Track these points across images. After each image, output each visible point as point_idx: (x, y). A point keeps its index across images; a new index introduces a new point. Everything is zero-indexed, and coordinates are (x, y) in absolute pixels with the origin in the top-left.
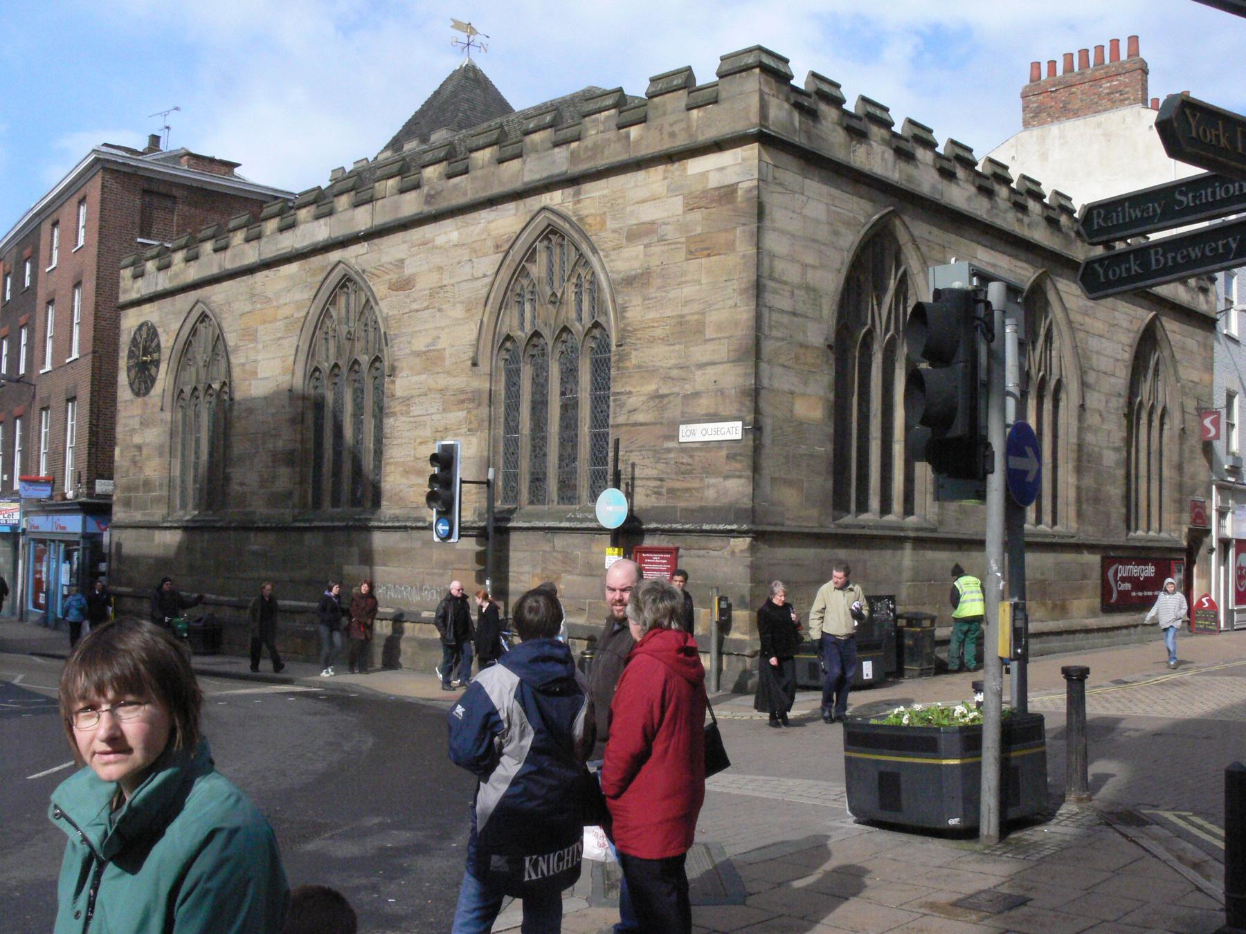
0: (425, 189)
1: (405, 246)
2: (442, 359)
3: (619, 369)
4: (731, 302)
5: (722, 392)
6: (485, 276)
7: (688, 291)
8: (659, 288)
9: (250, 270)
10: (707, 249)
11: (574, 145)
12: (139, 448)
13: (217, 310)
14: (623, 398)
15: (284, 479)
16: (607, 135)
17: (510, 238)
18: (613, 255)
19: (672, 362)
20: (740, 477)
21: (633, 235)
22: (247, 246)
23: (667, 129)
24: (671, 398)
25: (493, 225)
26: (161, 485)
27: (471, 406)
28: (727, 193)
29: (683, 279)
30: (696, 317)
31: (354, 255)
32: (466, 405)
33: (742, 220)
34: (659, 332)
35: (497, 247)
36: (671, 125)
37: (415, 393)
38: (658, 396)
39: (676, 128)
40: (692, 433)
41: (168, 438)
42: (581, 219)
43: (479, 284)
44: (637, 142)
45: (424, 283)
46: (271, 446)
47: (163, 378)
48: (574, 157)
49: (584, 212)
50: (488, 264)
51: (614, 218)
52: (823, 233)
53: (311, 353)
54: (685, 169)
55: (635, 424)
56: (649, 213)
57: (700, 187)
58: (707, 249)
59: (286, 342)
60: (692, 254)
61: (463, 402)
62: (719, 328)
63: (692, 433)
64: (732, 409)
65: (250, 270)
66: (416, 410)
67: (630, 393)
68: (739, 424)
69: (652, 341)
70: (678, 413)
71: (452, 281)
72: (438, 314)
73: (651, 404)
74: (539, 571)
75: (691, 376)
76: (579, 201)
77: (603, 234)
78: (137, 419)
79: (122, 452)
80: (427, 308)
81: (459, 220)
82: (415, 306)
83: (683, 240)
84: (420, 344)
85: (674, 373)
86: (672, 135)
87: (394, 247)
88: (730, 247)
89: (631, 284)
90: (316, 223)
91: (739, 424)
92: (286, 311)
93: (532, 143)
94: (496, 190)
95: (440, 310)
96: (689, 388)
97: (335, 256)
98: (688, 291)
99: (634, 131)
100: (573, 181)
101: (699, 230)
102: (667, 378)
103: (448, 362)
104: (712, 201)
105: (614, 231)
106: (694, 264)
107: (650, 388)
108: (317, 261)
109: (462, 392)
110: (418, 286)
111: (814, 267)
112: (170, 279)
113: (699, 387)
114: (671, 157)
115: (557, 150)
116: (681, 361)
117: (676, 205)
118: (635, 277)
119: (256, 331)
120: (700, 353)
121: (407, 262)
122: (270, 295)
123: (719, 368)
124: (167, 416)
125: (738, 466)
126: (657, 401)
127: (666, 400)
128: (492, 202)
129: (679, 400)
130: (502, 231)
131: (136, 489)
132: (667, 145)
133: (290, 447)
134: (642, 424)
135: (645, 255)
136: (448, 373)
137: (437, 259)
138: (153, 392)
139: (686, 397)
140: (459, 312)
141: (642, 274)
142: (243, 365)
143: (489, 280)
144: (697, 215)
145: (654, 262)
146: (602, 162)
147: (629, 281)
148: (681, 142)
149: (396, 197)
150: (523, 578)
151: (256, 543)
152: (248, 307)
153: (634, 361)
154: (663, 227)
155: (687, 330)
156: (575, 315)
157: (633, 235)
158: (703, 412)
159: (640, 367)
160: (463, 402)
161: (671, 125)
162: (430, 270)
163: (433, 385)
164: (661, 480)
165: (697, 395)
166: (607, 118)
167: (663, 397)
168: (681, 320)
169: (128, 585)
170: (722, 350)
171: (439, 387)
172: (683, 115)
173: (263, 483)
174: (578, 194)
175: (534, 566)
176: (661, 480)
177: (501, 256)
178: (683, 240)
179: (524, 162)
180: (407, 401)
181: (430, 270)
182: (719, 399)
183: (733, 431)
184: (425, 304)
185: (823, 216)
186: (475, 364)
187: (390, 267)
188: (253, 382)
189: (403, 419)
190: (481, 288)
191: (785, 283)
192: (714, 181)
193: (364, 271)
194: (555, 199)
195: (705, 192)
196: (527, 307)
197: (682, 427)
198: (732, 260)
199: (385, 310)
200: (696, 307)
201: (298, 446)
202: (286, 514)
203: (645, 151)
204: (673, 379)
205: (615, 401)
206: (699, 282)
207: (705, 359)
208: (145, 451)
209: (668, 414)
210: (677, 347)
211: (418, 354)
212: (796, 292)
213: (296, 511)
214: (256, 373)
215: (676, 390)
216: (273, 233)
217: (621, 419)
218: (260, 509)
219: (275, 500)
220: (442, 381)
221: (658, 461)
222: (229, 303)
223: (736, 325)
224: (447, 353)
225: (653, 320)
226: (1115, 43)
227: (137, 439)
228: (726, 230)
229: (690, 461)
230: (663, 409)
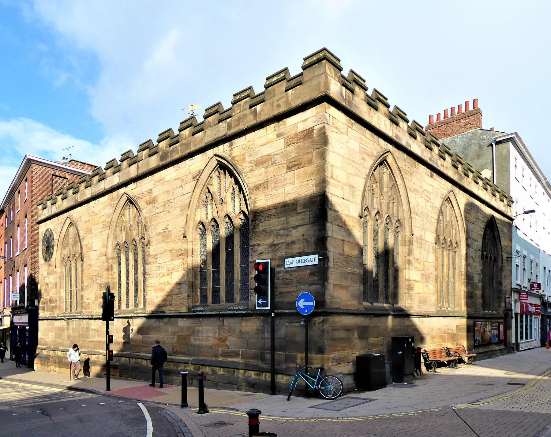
0: (160, 153)
1: (153, 182)
3: (253, 233)
6: (188, 193)
10: (298, 165)
12: (47, 285)
13: (75, 221)
14: (255, 247)
17: (200, 172)
18: (249, 174)
24: (280, 245)
25: (191, 167)
28: (308, 133)
29: (285, 183)
31: (130, 189)
34: (273, 212)
35: (194, 178)
38: (274, 245)
40: (292, 263)
42: (233, 158)
43: (185, 197)
45: (161, 200)
47: (57, 254)
51: (250, 155)
52: (357, 157)
56: (266, 151)
58: (298, 165)
59: (104, 233)
60: (289, 168)
63: (292, 263)
67: (259, 244)
69: (270, 217)
70: (283, 253)
71: (174, 197)
72: (168, 214)
73: (270, 249)
75: (290, 233)
77: (244, 165)
78: (46, 272)
82: (157, 211)
83: (285, 162)
85: (282, 232)
87: (147, 183)
88: (310, 162)
92: (103, 219)
94: (193, 149)
96: (289, 239)
97: (122, 190)
101: (293, 155)
107: (269, 241)
111: (353, 175)
113: (294, 239)
116: (285, 226)
118: (261, 185)
122: (96, 212)
126: (273, 247)
127: (277, 247)
128: (191, 155)
129: (284, 246)
131: (47, 303)
135: (266, 173)
137: (166, 187)
138: (52, 260)
139: (288, 244)
140: (176, 212)
141: (264, 182)
143: (190, 195)
146: (243, 126)
147: (257, 187)
152: (88, 218)
153: (261, 228)
154: (275, 156)
158: (297, 251)
159: (264, 231)
162: (164, 193)
165: (293, 243)
167: (275, 245)
169: (45, 345)
174: (231, 145)
177: (196, 181)
178: (285, 162)
181: (164, 193)
182: (306, 244)
183: (313, 260)
184: (162, 209)
185: (357, 149)
191: (339, 182)
193: (135, 196)
194: (221, 149)
196: (209, 206)
197: (286, 260)
199: (145, 214)
204: (281, 235)
206: (294, 183)
207: (297, 224)
209: (279, 254)
210: (282, 219)
211: (159, 234)
212: (344, 187)
214: (92, 248)
215: (283, 241)
222: (80, 217)
226: (467, 103)
227: (47, 281)
229: (290, 277)
230: (276, 251)
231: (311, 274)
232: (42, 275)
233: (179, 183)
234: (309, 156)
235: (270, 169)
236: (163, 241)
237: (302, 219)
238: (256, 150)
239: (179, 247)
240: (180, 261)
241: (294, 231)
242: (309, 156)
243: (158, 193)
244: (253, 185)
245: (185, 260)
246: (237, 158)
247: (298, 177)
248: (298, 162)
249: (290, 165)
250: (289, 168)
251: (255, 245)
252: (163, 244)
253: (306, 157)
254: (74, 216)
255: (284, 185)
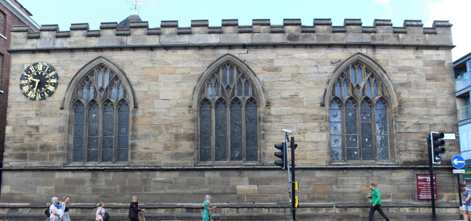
2: (303, 102)
3: (399, 113)
4: (446, 97)
5: (445, 124)
6: (326, 73)
7: (428, 91)
8: (415, 89)
9: (152, 48)
10: (434, 79)
11: (372, 34)
12: (37, 128)
13: (119, 64)
14: (403, 123)
15: (186, 146)
16: (389, 34)
17: (340, 61)
18: (393, 75)
19: (423, 113)
20: (455, 151)
21: (401, 70)
22: (148, 37)
23: (415, 38)
24: (424, 125)
25: (329, 55)
26: (62, 148)
27: (321, 121)
30: (432, 100)
32: (317, 121)
33: (448, 72)
34: (417, 103)
36: (418, 37)
37: (284, 114)
39: (419, 38)
41: (68, 124)
44: (403, 39)
46: (174, 131)
48: (373, 38)
49: (378, 58)
50: (329, 69)
51: (392, 62)
53: (203, 91)
54: (422, 52)
55: (409, 133)
56: (407, 64)
57: (430, 59)
58: (434, 79)
61: (316, 119)
62: (442, 104)
64: (449, 130)
65: (152, 48)
66: (286, 121)
67: (405, 122)
68: (454, 134)
69: (414, 106)
71: (305, 72)
72: (297, 84)
73: (416, 126)
74: (365, 183)
76: (375, 54)
77: (388, 67)
78: (34, 112)
79: (14, 130)
80: (291, 81)
81: (309, 50)
83: (424, 75)
84: (286, 94)
85: (425, 117)
86: (418, 40)
88: (444, 80)
89: (402, 86)
90: (208, 35)
91: (454, 134)
92: (184, 71)
93: (350, 28)
95: (298, 82)
96: (431, 122)
98: (428, 91)
99: (401, 36)
100: (374, 47)
101: (431, 72)
102: (421, 118)
103: (305, 103)
104: (435, 64)
105: (393, 67)
106: (429, 83)
107: (415, 121)
108: (208, 52)
109: (315, 115)
110: (283, 72)
112: (70, 43)
113: (435, 122)
114: (418, 47)
115: (364, 34)
117: (420, 63)
118: (404, 84)
119: (158, 77)
120: (434, 111)
121: (275, 61)
123: (444, 117)
124: (66, 112)
125: (454, 147)
126: (418, 125)
127: (422, 125)
128: (330, 46)
129: (428, 126)
130: (335, 58)
132: (416, 43)
133: (191, 132)
134: (412, 133)
135: (408, 77)
136: (306, 107)
137: (295, 63)
140: (311, 84)
141: (407, 83)
142: (146, 92)
144: (430, 68)
145: (412, 80)
147: (402, 85)
148: (421, 43)
149: (268, 34)
150: (356, 187)
151: (160, 177)
152: (151, 65)
155: (426, 103)
156: (373, 93)
157: (401, 70)
159: (409, 114)
160: (316, 119)
161: (418, 37)
163: (296, 111)
164: (422, 151)
165: (435, 124)
166: (388, 28)
167: (420, 124)
168: (426, 100)
170: (444, 112)
171: (301, 112)
172: (423, 35)
173: (166, 148)
174: (374, 51)
175: (363, 182)
176: (422, 151)
179: (347, 35)
180: (280, 117)
181: (291, 66)
182: (445, 127)
184: (290, 79)
186: (323, 105)
187: (263, 61)
188: (156, 101)
189: (277, 124)
190: (325, 78)
192: (435, 58)
193: (245, 60)
195: (432, 61)
198: (445, 84)
199: (261, 79)
200: (432, 97)
201: (196, 132)
202: (189, 163)
203: (405, 43)
205: (398, 124)
207: (437, 113)
208: (42, 130)
210: (425, 109)
211: (285, 99)
213: (196, 162)
214: (158, 96)
215: (426, 122)
216: (171, 34)
217: (402, 130)
218: (163, 160)
219: (176, 156)
220: (302, 110)
221: (421, 145)
223: (449, 104)
224: (305, 100)
225: (414, 99)
228: (442, 74)
230: (421, 128)
231: (450, 145)
232: (17, 115)
233: (314, 63)
234: (443, 76)
235: (411, 76)
236: (290, 105)
237: (441, 111)
238: (399, 61)
239: (316, 113)
240: (318, 124)
241: (435, 118)
242: (443, 76)
243: (283, 65)
244: (398, 82)
245: (323, 124)
246: (381, 61)
247: (436, 86)
248: (434, 77)
249: (429, 78)
250: (427, 79)
251: (402, 122)
252: (291, 108)
253: (440, 76)
254: (114, 57)
255: (424, 88)
